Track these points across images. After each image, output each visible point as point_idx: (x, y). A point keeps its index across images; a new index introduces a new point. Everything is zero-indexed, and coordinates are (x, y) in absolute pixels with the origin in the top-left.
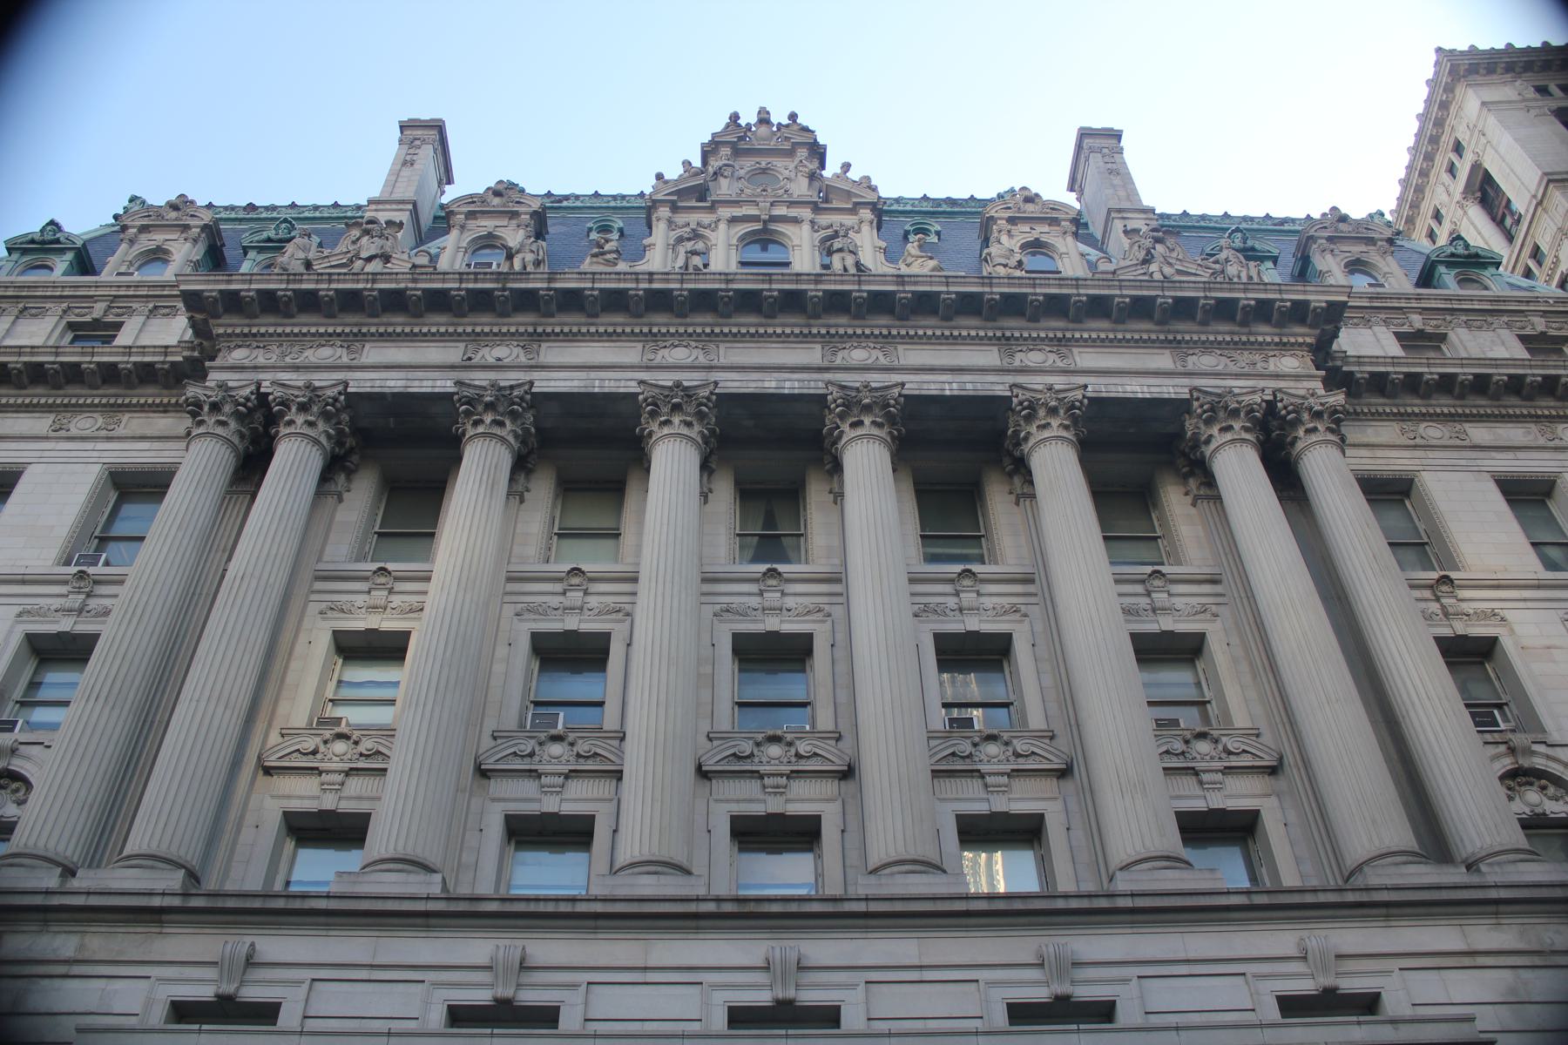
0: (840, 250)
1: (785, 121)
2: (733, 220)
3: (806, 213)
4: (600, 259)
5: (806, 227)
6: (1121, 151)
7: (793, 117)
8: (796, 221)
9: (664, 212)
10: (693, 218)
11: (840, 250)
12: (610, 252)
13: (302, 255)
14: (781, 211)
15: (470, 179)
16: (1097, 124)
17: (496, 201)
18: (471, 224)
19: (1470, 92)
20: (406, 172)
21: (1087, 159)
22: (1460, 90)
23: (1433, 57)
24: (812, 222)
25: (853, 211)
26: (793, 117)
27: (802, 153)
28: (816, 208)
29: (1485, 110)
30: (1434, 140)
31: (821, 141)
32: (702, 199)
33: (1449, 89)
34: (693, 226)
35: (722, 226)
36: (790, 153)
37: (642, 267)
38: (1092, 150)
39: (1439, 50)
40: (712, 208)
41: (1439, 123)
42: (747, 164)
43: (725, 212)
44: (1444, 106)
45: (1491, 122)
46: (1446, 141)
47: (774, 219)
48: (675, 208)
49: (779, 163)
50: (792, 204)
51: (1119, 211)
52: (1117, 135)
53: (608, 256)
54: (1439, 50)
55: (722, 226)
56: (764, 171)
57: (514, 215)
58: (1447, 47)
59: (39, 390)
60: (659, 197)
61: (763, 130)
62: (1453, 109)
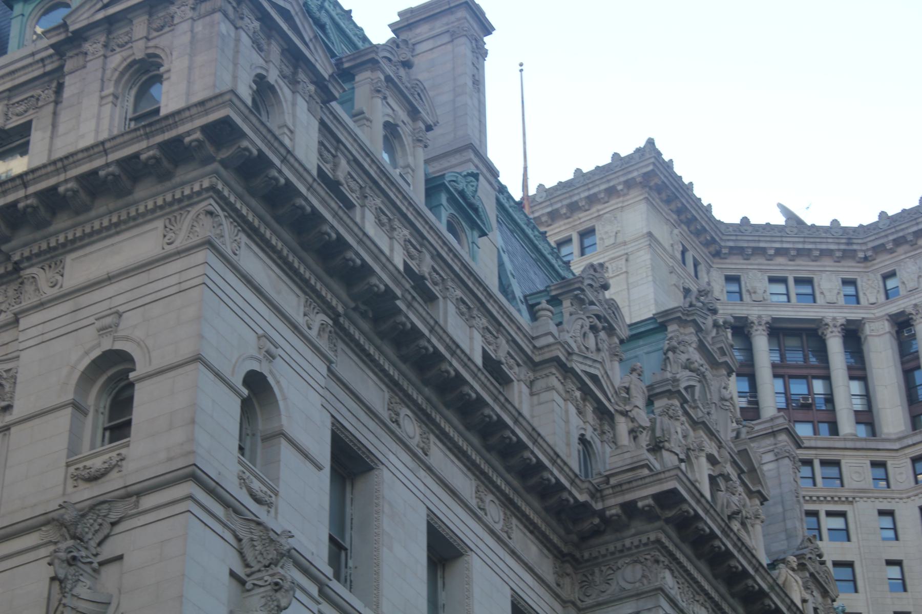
19: (643, 207)
22: (636, 195)
23: (642, 144)
29: (645, 242)
30: (574, 208)
33: (629, 184)
39: (651, 142)
41: (592, 200)
44: (611, 192)
45: (644, 257)
46: (583, 220)
47: (727, 478)
54: (651, 142)
55: (703, 460)
58: (658, 145)
59: (476, 441)
62: (614, 203)
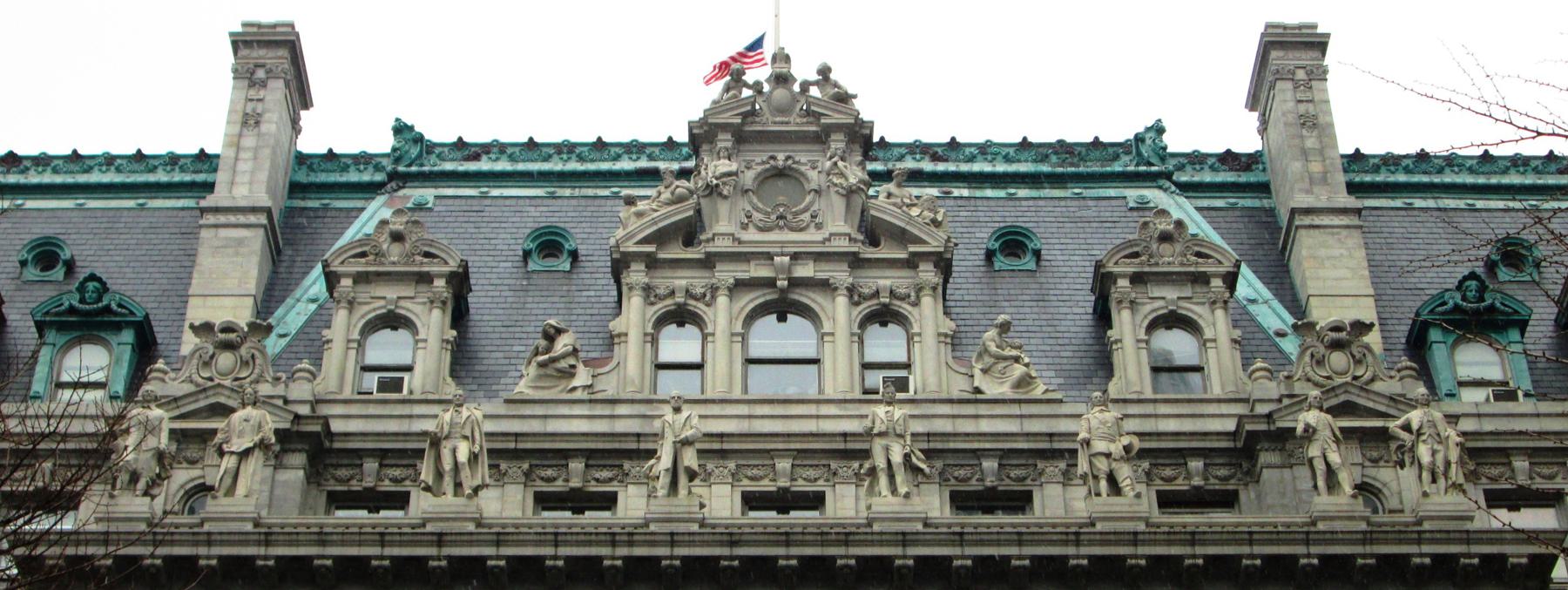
0: (881, 434)
1: (814, 77)
2: (740, 285)
3: (840, 275)
4: (549, 371)
5: (842, 301)
6: (1320, 74)
7: (825, 72)
8: (825, 286)
9: (636, 275)
10: (681, 280)
11: (881, 434)
12: (564, 356)
13: (152, 442)
14: (805, 270)
15: (344, 123)
16: (1292, 17)
17: (395, 252)
18: (365, 293)
20: (249, 141)
21: (1272, 87)
24: (851, 290)
25: (911, 263)
26: (825, 72)
27: (837, 143)
28: (856, 262)
31: (865, 116)
32: (689, 242)
34: (680, 299)
35: (722, 300)
36: (820, 138)
37: (609, 386)
38: (1279, 76)
40: (709, 262)
42: (759, 158)
43: (726, 274)
48: (652, 263)
49: (803, 157)
50: (819, 257)
51: (1308, 211)
52: (1317, 44)
53: (563, 364)
56: (781, 173)
57: (425, 279)
60: (631, 247)
61: (780, 94)
